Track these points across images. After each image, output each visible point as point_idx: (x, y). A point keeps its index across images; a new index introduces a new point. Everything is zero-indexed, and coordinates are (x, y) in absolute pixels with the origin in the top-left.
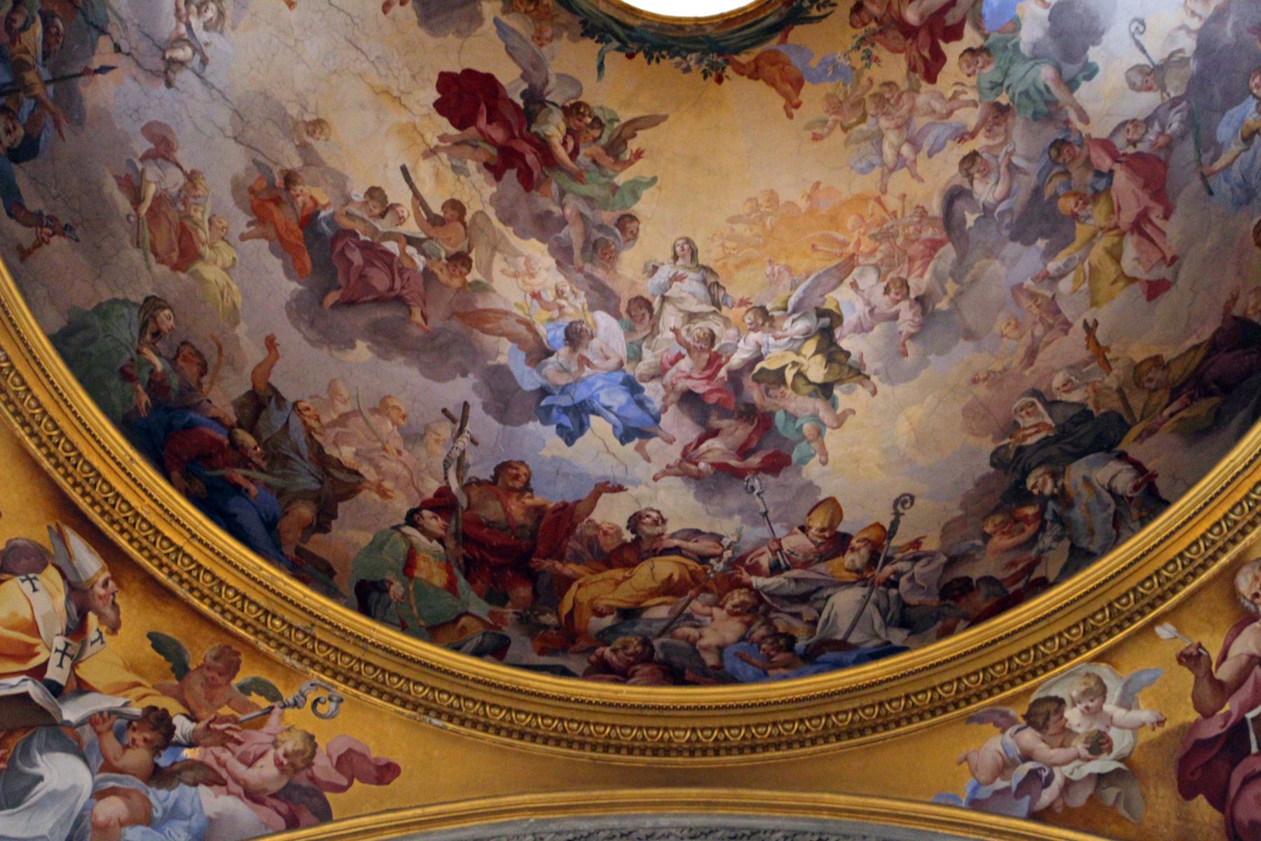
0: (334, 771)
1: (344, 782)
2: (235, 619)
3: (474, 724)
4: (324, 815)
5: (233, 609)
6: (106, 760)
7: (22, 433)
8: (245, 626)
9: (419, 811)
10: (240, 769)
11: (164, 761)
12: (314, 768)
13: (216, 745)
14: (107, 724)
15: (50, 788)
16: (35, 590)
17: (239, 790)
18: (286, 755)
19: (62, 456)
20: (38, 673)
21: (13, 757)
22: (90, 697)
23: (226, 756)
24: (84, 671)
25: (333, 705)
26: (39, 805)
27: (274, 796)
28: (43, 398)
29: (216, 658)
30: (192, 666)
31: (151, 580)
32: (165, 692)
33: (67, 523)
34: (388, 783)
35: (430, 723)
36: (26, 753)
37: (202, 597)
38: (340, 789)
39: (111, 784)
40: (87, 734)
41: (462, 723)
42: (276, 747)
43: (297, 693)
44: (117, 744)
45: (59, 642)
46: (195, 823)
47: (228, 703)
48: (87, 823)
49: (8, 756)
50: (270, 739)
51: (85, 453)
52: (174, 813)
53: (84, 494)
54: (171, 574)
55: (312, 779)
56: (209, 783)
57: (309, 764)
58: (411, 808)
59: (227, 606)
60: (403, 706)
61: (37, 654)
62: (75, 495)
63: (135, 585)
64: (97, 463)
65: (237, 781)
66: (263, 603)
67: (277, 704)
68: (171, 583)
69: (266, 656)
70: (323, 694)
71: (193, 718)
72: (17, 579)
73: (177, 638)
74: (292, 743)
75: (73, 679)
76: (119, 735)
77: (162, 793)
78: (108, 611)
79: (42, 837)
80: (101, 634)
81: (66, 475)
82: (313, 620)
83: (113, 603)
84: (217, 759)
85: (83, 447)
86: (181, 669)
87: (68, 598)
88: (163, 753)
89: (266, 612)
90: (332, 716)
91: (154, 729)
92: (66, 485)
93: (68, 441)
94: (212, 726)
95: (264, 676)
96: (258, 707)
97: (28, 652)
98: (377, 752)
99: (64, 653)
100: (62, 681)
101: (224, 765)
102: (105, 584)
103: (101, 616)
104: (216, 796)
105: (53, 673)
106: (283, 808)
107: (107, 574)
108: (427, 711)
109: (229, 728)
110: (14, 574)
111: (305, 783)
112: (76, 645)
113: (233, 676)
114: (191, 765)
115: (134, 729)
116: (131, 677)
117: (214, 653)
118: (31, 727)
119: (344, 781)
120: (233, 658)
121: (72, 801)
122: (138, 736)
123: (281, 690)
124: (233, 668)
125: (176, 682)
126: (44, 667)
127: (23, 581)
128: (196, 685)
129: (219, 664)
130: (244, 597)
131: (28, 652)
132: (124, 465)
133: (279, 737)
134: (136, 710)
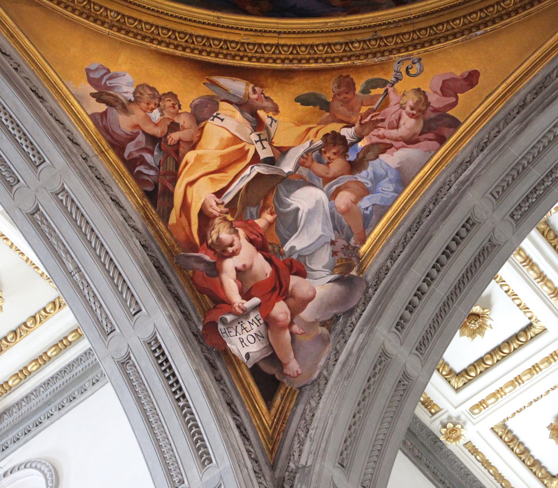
0: (444, 98)
1: (454, 100)
2: (333, 60)
3: (501, 18)
4: (455, 124)
5: (328, 55)
6: (323, 177)
7: (154, 46)
8: (341, 59)
9: (504, 85)
10: (394, 133)
11: (352, 157)
12: (432, 104)
13: (372, 130)
14: (310, 159)
15: (306, 211)
16: (222, 120)
17: (401, 143)
18: (412, 109)
19: (182, 42)
20: (256, 159)
21: (276, 208)
23: (382, 132)
24: (279, 142)
25: (417, 66)
27: (422, 133)
28: (151, 20)
29: (339, 87)
30: (330, 100)
32: (326, 123)
33: (212, 75)
34: (477, 83)
35: (476, 35)
36: (281, 202)
37: (308, 61)
39: (334, 187)
40: (303, 171)
41: (494, 22)
42: (404, 109)
43: (394, 73)
44: (322, 166)
45: (254, 137)
46: (391, 176)
47: (362, 104)
49: (274, 209)
50: (398, 107)
51: (193, 32)
52: (377, 179)
53: (209, 54)
54: (283, 61)
55: (435, 110)
56: (383, 152)
57: (428, 104)
58: (498, 87)
59: (324, 56)
60: (455, 38)
61: (248, 150)
62: (204, 57)
63: (269, 81)
64: (202, 33)
65: (396, 140)
66: (341, 40)
67: (387, 87)
68: (287, 65)
69: (363, 66)
70: (409, 63)
71: (350, 125)
72: (209, 121)
73: (311, 91)
74: (411, 99)
75: (274, 149)
76: (320, 161)
77: (364, 173)
78: (266, 104)
79: (321, 236)
80: (271, 117)
81: (192, 51)
82: (373, 29)
83: (266, 97)
84: (378, 136)
85: (189, 30)
86: (325, 106)
87: (241, 112)
88: (348, 153)
89: (347, 44)
91: (335, 145)
92: (196, 56)
93: (179, 33)
94: (362, 122)
95: (370, 77)
96: (379, 95)
97: (243, 153)
98: (458, 72)
99: (261, 140)
100: (272, 155)
101: (384, 137)
102: (254, 91)
103: (264, 109)
104: (392, 155)
105: (263, 155)
106: (431, 135)
107: (251, 85)
108: (470, 31)
109: (372, 117)
111: (433, 115)
113: (355, 89)
114: (367, 149)
115: (325, 152)
116: (304, 128)
117: (336, 85)
118: (274, 187)
120: (347, 80)
121: (321, 209)
122: (328, 155)
123: (385, 78)
124: (351, 86)
125: (328, 114)
126: (256, 154)
127: (213, 120)
128: (340, 108)
129: (343, 89)
130: (329, 45)
131: (243, 153)
132: (216, 24)
133: (401, 102)
134: (319, 142)
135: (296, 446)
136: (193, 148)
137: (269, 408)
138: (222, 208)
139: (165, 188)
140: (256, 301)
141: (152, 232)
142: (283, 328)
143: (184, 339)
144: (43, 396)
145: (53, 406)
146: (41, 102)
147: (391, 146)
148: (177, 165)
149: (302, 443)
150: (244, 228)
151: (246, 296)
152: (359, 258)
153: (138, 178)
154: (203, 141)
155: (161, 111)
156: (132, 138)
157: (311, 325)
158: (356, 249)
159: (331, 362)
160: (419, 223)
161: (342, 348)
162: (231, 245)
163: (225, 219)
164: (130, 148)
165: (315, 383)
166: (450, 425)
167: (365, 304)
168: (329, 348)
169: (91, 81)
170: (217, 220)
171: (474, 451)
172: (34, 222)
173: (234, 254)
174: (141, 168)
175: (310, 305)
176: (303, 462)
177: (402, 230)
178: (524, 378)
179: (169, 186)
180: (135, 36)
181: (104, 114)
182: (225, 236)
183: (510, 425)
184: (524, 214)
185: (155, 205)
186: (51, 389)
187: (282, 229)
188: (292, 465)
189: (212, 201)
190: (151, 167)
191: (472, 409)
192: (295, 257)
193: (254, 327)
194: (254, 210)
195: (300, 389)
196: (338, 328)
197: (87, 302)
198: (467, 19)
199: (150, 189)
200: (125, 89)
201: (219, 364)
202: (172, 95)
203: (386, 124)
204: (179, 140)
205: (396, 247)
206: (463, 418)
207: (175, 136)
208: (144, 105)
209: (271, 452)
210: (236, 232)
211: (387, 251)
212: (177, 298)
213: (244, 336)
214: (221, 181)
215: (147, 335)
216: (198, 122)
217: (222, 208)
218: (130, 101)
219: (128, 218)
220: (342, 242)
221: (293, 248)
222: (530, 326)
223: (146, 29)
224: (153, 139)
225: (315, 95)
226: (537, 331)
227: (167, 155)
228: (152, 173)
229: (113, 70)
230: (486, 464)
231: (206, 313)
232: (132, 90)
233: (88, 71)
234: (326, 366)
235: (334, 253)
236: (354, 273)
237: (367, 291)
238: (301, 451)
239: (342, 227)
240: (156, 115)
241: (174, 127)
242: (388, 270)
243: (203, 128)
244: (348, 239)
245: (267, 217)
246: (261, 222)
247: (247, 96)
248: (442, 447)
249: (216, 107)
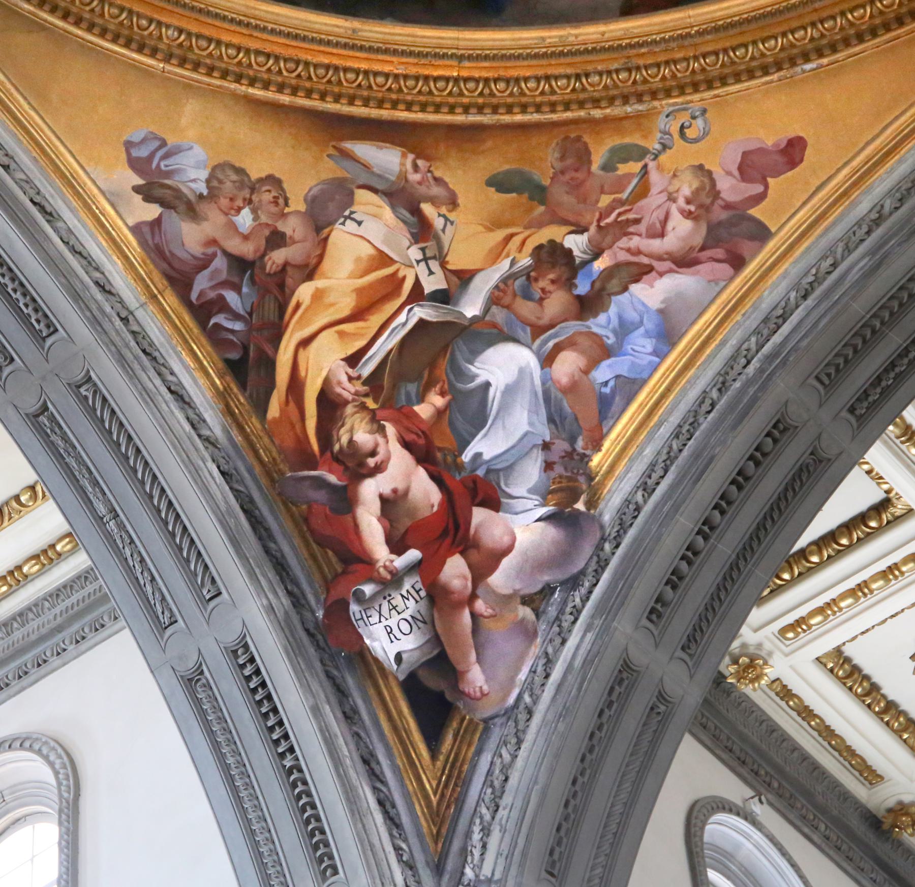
0: (744, 184)
1: (760, 188)
2: (553, 106)
3: (847, 43)
4: (762, 234)
5: (545, 99)
6: (532, 326)
8: (567, 107)
9: (846, 171)
10: (656, 245)
11: (583, 287)
12: (722, 195)
13: (618, 239)
14: (510, 292)
15: (502, 387)
16: (360, 223)
17: (668, 265)
18: (688, 202)
20: (417, 295)
21: (450, 383)
22: (477, 281)
23: (635, 242)
24: (456, 262)
25: (700, 122)
26: (505, 407)
27: (703, 248)
28: (236, 40)
29: (562, 158)
30: (546, 182)
31: (452, 128)
32: (540, 224)
33: (342, 139)
34: (802, 161)
35: (804, 71)
37: (509, 109)
38: (760, 198)
39: (551, 344)
40: (499, 315)
41: (834, 49)
42: (674, 200)
43: (659, 135)
44: (531, 304)
45: (415, 253)
46: (649, 324)
47: (602, 192)
48: (555, 393)
49: (446, 386)
50: (663, 197)
51: (309, 58)
53: (337, 98)
55: (728, 206)
56: (637, 281)
57: (715, 194)
58: (839, 170)
59: (538, 99)
60: (766, 73)
61: (404, 278)
62: (330, 106)
63: (442, 147)
65: (660, 258)
66: (569, 71)
67: (647, 160)
68: (474, 118)
69: (606, 120)
70: (684, 118)
71: (580, 230)
72: (337, 226)
73: (513, 166)
74: (686, 187)
75: (447, 273)
76: (527, 296)
77: (602, 318)
78: (436, 190)
79: (526, 434)
80: (444, 216)
81: (309, 94)
82: (626, 53)
83: (436, 179)
84: (629, 250)
86: (539, 193)
87: (393, 207)
88: (577, 281)
89: (578, 77)
90: (706, 134)
91: (554, 265)
93: (286, 60)
94: (602, 224)
97: (395, 282)
99: (426, 259)
100: (443, 286)
101: (638, 252)
102: (416, 168)
103: (433, 200)
104: (652, 286)
105: (430, 285)
106: (719, 253)
107: (411, 157)
108: (793, 62)
109: (620, 214)
110: (331, 223)
111: (724, 215)
112: (431, 244)
113: (590, 162)
114: (609, 273)
115: (536, 280)
116: (500, 235)
117: (557, 155)
118: (447, 346)
119: (759, 188)
120: (578, 145)
121: (528, 384)
122: (543, 283)
123: (642, 143)
124: (584, 157)
125: (542, 209)
126: (417, 284)
127: (343, 224)
128: (561, 196)
129: (569, 162)
130: (547, 78)
131: (395, 282)
132: (351, 42)
133: (671, 189)
134: (525, 261)
135: (476, 836)
136: (310, 277)
137: (434, 754)
138: (359, 387)
139: (261, 352)
140: (413, 555)
141: (239, 439)
142: (458, 606)
143: (294, 650)
144: (50, 616)
145: (67, 633)
146: (48, 221)
147: (649, 269)
148: (282, 309)
149: (486, 831)
150: (395, 422)
151: (397, 547)
152: (590, 478)
153: (215, 336)
154: (326, 264)
155: (254, 211)
156: (204, 263)
157: (506, 600)
158: (585, 458)
159: (538, 680)
160: (695, 424)
161: (557, 651)
162: (373, 453)
163: (363, 407)
164: (202, 283)
165: (509, 713)
166: (744, 660)
167: (598, 574)
168: (535, 650)
169: (135, 164)
170: (349, 409)
171: (786, 693)
172: (40, 430)
173: (379, 469)
174: (219, 319)
175: (506, 562)
176: (486, 871)
177: (666, 431)
178: (874, 586)
179: (269, 350)
180: (210, 71)
181: (157, 223)
182: (363, 437)
183: (848, 651)
184: (873, 407)
185: (243, 386)
186: (62, 606)
187: (460, 423)
188: (469, 872)
189: (342, 373)
190: (236, 317)
191: (783, 631)
192: (480, 473)
193: (411, 603)
194: (412, 388)
195: (486, 721)
196: (552, 611)
197: (130, 570)
198: (787, 37)
199: (234, 355)
200: (193, 174)
201: (351, 682)
202: (273, 181)
203: (642, 228)
204: (286, 264)
205: (652, 466)
206: (767, 646)
207: (278, 257)
208: (224, 202)
209: (436, 838)
210: (382, 430)
211: (640, 467)
212: (280, 567)
213: (392, 622)
214: (355, 336)
215: (231, 637)
216: (318, 229)
217: (359, 387)
218: (201, 197)
219: (197, 422)
220: (561, 446)
221: (478, 455)
222: (884, 504)
223: (228, 56)
224: (240, 264)
225: (520, 173)
226: (898, 512)
227: (263, 292)
228: (238, 326)
229: (171, 141)
230: (806, 713)
231: (328, 585)
232: (204, 174)
233: (129, 145)
234: (529, 686)
235: (548, 466)
236: (580, 506)
237: (599, 548)
238: (484, 846)
239: (563, 418)
240: (245, 219)
241: (277, 239)
242: (638, 509)
243: (326, 239)
244: (572, 440)
245: (436, 400)
246: (424, 411)
247: (403, 176)
248: (729, 691)
249: (349, 200)
